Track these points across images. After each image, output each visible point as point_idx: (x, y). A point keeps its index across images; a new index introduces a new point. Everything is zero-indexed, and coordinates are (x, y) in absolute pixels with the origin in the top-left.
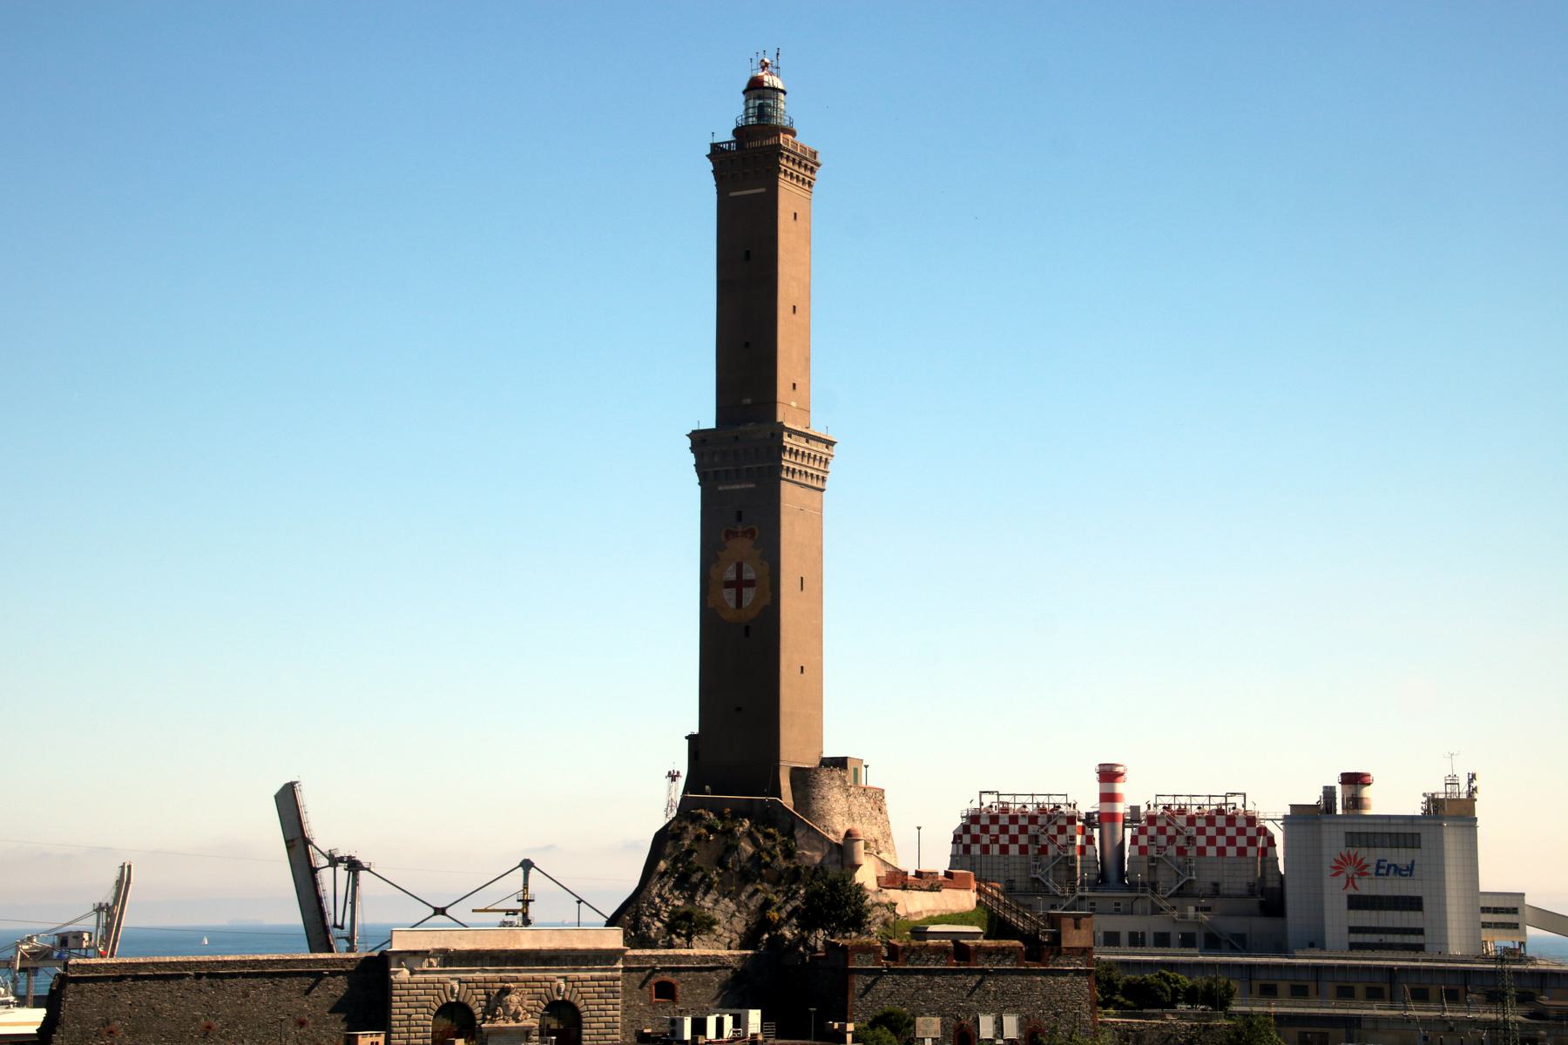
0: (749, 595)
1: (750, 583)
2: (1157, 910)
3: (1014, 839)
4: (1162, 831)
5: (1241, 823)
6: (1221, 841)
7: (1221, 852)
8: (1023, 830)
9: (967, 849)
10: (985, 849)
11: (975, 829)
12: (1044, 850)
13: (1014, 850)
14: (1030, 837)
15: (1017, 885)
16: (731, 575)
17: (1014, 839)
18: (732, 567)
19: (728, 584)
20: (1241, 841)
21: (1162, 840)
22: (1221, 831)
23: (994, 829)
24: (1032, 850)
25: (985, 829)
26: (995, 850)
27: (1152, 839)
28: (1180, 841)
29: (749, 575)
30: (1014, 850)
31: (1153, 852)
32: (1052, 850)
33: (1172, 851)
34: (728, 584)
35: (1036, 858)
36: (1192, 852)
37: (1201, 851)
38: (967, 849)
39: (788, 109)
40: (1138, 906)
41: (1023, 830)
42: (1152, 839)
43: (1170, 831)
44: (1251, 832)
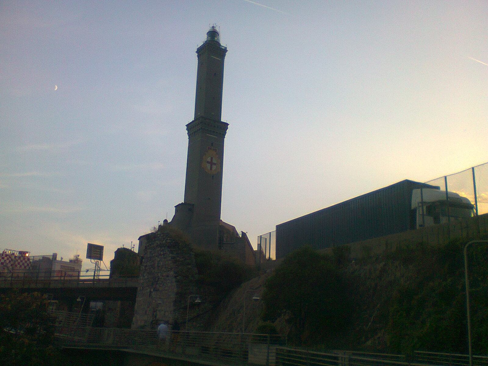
0: (214, 167)
1: (215, 164)
4: (8, 259)
5: (26, 260)
6: (21, 264)
7: (21, 266)
16: (209, 159)
18: (210, 158)
19: (208, 162)
20: (26, 264)
21: (8, 261)
22: (21, 261)
27: (5, 261)
28: (12, 263)
29: (214, 161)
33: (9, 265)
34: (208, 162)
37: (16, 266)
39: (223, 42)
42: (5, 261)
43: (10, 259)
44: (28, 262)
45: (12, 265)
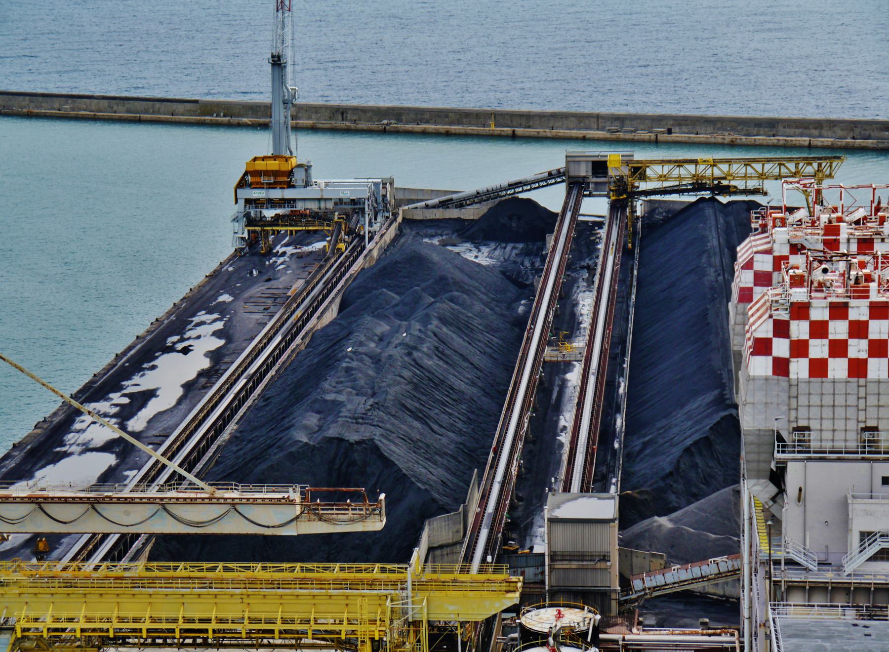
9: (781, 367)
10: (818, 368)
11: (800, 330)
23: (839, 329)
26: (838, 368)
38: (781, 367)
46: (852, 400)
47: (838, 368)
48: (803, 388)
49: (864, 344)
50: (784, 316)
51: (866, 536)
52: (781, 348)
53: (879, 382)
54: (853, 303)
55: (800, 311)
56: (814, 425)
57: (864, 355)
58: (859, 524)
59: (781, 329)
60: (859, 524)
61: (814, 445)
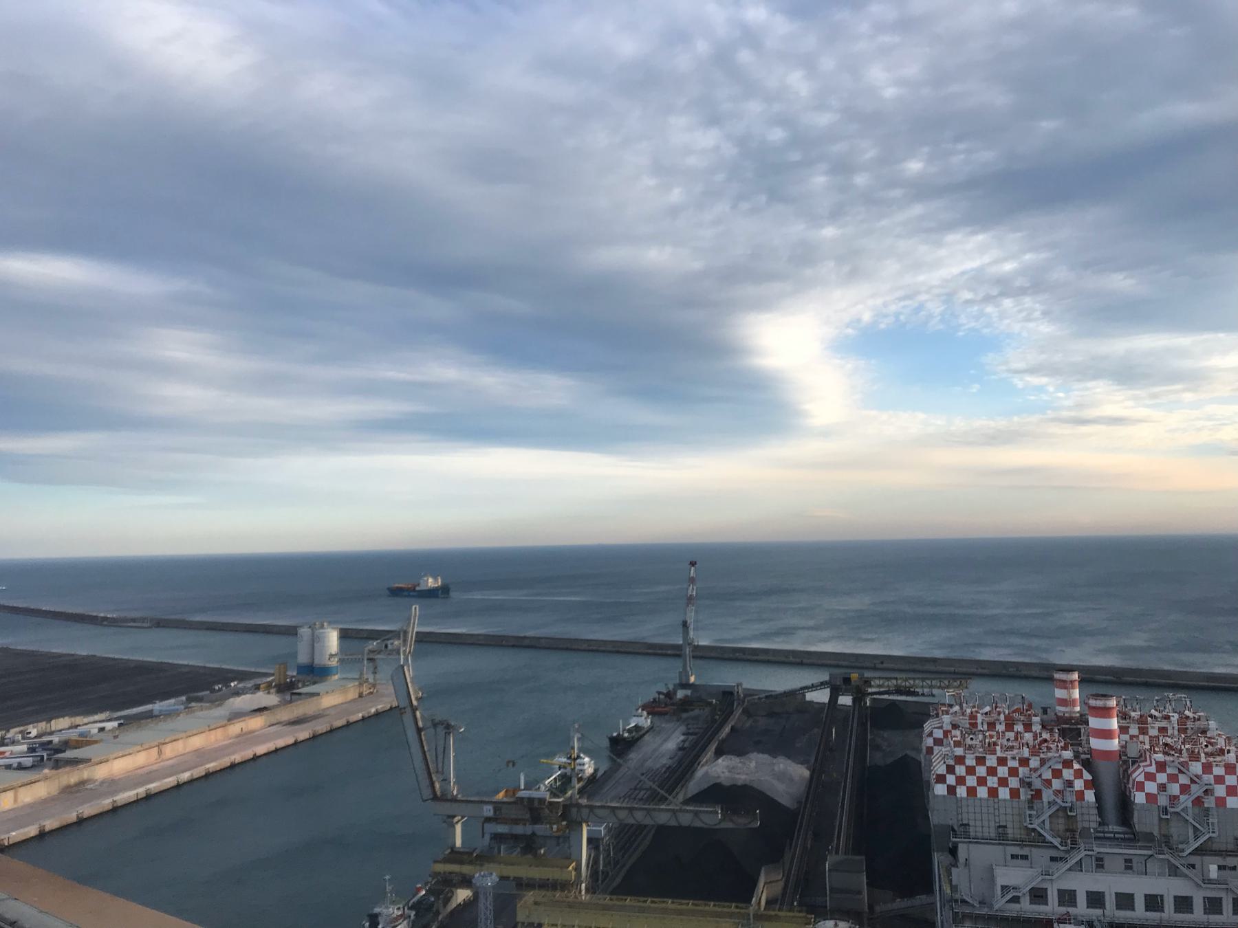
2: (1174, 872)
3: (1003, 782)
8: (1014, 772)
9: (952, 790)
11: (960, 770)
12: (1038, 794)
13: (1004, 793)
14: (1022, 781)
15: (1010, 831)
17: (1003, 782)
21: (1175, 789)
23: (981, 771)
24: (1024, 795)
25: (971, 771)
26: (982, 792)
28: (1196, 790)
30: (1004, 793)
31: (1163, 801)
32: (1047, 795)
33: (1186, 801)
35: (1031, 803)
36: (1209, 802)
38: (952, 790)
40: (1152, 866)
41: (1014, 772)
43: (1183, 780)
45: (1198, 802)
46: (991, 810)
47: (982, 792)
48: (964, 803)
49: (995, 779)
50: (952, 762)
51: (1003, 887)
52: (951, 779)
53: (1005, 800)
54: (988, 757)
55: (960, 760)
56: (972, 823)
57: (996, 785)
58: (1000, 881)
59: (951, 769)
60: (1000, 881)
61: (972, 834)
